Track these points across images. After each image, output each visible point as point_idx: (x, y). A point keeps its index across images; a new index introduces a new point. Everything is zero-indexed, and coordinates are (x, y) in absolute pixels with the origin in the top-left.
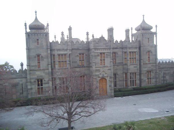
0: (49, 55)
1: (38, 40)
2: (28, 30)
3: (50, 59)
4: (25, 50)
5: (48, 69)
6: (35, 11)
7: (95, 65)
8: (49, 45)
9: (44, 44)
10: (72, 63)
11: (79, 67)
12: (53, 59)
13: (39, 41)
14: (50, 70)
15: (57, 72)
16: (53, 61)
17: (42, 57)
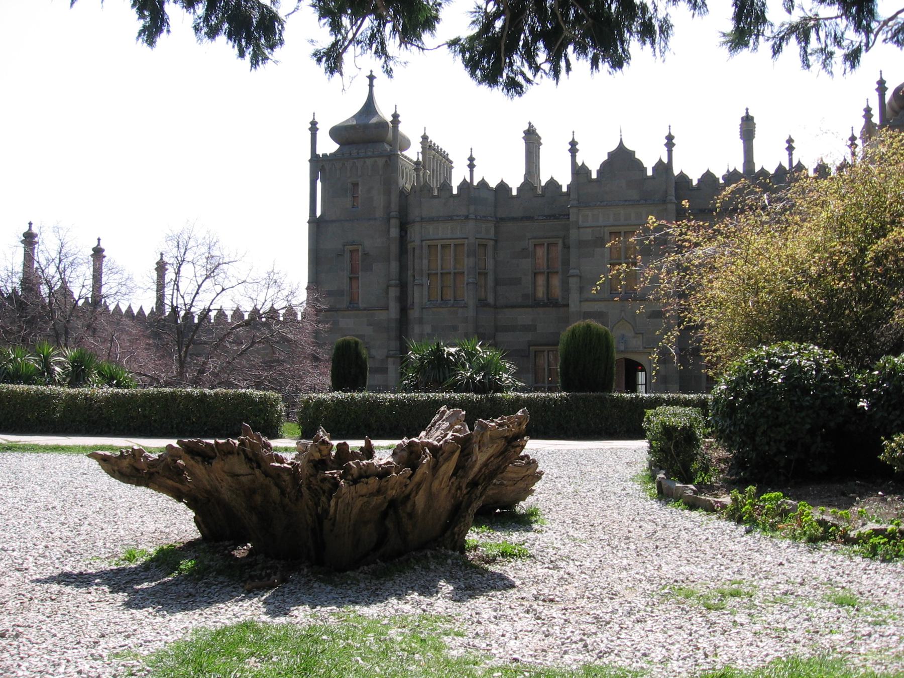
0: (394, 249)
1: (355, 185)
2: (328, 146)
3: (394, 266)
4: (305, 228)
5: (387, 309)
6: (369, 74)
7: (581, 289)
8: (394, 207)
9: (379, 201)
10: (497, 282)
11: (531, 307)
12: (410, 263)
13: (360, 188)
14: (394, 312)
15: (421, 321)
16: (410, 272)
17: (366, 255)
